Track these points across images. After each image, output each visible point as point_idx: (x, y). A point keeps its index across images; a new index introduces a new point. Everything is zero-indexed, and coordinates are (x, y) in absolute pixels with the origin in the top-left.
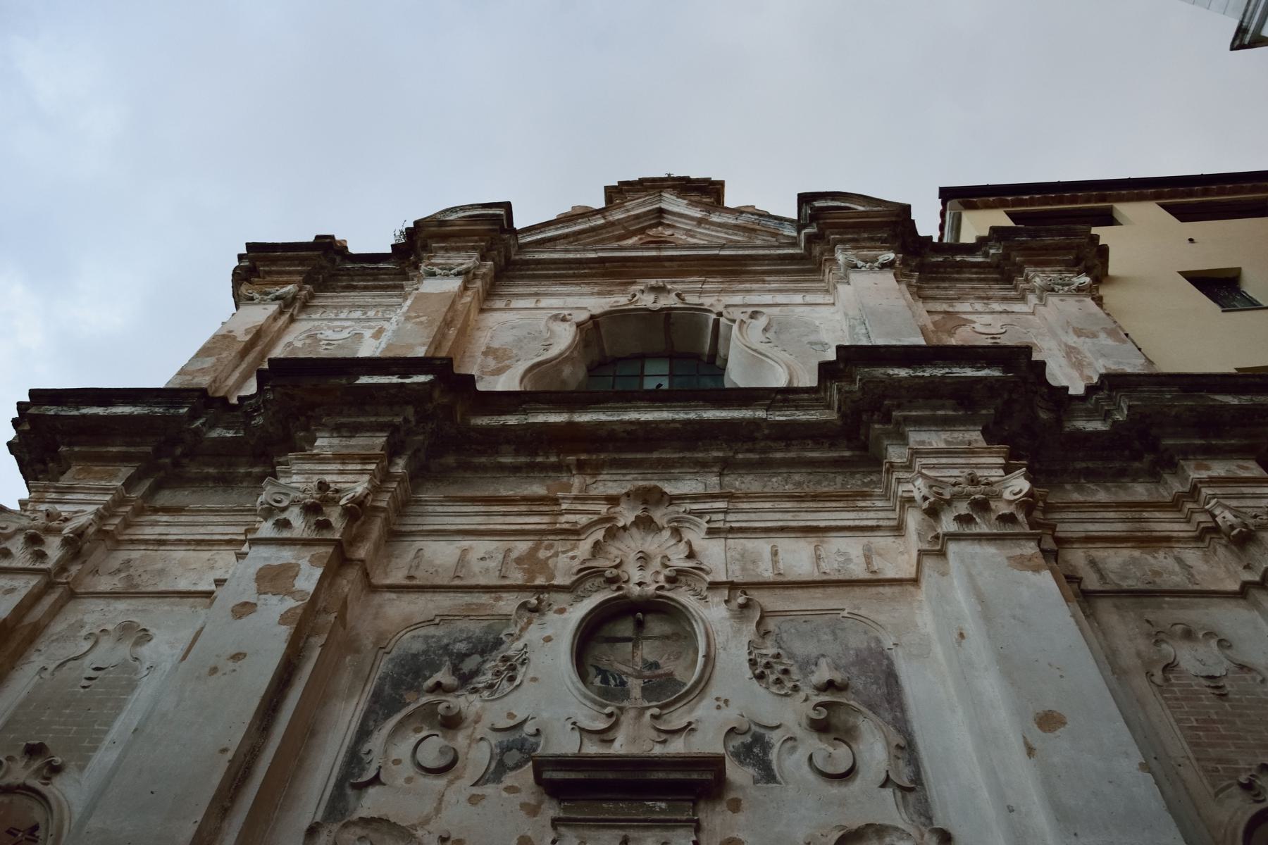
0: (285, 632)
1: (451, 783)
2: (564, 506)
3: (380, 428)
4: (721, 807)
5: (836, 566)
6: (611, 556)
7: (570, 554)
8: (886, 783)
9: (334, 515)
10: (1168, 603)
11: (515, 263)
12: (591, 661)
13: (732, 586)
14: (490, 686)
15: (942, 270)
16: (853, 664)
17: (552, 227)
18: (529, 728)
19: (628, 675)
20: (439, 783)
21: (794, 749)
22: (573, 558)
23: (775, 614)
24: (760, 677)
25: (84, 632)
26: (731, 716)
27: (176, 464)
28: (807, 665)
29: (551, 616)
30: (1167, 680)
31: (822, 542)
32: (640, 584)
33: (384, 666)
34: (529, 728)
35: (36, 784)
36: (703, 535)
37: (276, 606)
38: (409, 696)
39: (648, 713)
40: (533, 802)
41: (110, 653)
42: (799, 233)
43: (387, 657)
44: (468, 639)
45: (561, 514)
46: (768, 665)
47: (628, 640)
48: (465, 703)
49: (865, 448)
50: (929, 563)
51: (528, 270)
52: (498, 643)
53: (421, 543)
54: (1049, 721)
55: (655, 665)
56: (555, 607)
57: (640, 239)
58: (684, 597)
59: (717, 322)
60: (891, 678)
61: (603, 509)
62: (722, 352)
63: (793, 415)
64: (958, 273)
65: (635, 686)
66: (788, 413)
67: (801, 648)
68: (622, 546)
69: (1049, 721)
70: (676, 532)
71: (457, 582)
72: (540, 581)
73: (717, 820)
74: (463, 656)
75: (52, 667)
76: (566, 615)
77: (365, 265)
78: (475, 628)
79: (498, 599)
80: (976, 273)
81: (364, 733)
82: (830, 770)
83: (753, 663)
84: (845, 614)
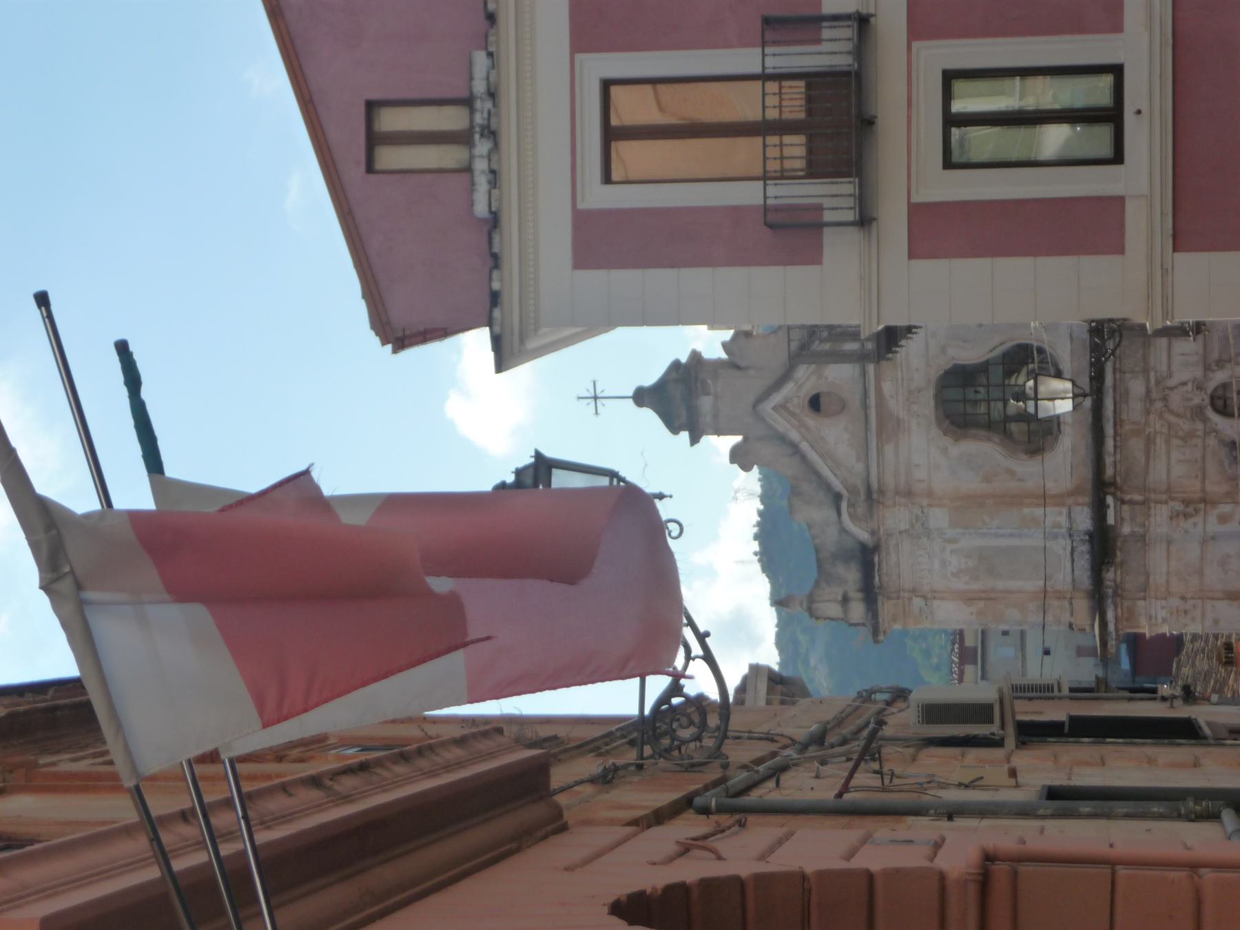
9: (1190, 510)
22: (1184, 423)
29: (1219, 427)
58: (1211, 386)
61: (1152, 417)
72: (1200, 433)
78: (1224, 452)
79: (1209, 446)
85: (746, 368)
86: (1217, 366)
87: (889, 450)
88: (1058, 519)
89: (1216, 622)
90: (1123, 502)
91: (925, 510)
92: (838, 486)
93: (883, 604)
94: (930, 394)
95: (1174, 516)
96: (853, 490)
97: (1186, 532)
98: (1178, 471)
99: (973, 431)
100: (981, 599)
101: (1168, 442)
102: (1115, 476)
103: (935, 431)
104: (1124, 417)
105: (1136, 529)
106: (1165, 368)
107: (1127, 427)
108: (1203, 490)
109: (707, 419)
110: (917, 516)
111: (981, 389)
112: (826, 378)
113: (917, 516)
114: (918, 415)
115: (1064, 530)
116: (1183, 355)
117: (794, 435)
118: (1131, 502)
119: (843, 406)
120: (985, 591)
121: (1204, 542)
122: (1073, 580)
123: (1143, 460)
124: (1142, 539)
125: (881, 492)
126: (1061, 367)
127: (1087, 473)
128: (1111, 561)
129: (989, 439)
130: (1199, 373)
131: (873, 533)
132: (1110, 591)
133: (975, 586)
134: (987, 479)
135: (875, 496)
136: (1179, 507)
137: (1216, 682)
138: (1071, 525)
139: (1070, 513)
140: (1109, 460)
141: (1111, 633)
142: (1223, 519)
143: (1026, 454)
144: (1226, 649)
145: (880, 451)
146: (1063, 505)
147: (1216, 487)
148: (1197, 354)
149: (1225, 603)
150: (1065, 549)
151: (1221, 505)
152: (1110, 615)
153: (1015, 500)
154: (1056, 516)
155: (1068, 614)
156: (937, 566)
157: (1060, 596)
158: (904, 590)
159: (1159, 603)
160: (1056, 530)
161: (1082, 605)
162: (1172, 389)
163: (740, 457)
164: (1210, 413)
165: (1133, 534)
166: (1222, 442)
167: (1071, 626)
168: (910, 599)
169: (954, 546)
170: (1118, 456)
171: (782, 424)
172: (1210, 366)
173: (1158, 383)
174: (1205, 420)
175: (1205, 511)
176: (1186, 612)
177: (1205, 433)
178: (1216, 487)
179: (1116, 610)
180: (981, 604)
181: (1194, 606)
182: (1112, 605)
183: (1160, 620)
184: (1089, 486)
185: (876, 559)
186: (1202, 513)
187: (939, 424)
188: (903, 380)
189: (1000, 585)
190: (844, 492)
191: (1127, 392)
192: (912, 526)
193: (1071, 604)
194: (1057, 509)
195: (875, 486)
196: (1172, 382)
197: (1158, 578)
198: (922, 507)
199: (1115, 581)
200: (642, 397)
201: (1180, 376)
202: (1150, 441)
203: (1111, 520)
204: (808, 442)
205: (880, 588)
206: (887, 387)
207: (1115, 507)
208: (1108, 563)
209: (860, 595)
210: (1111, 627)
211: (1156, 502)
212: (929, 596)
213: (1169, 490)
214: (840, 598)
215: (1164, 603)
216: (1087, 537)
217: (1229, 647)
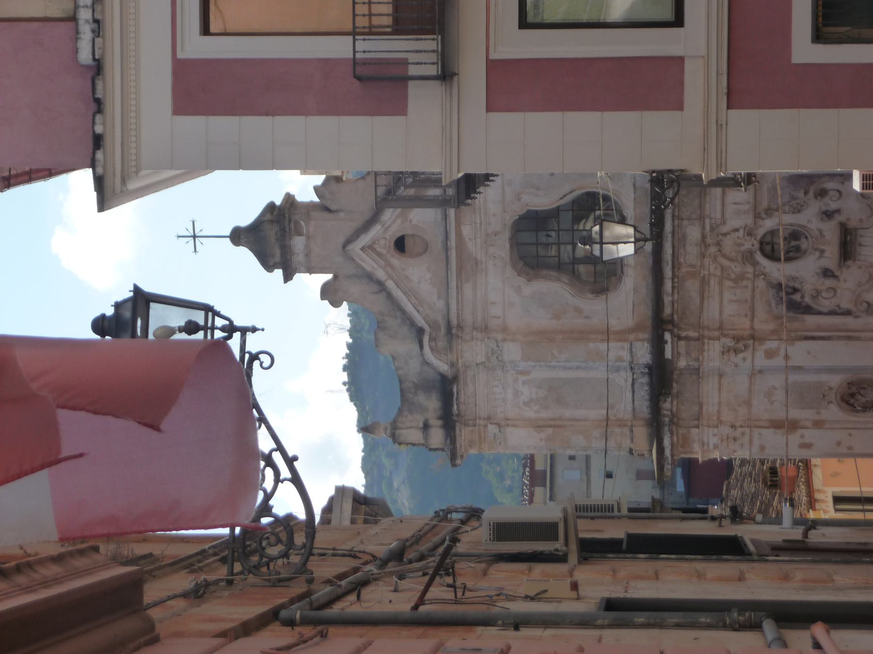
7: (733, 268)
8: (843, 183)
9: (740, 345)
20: (839, 291)
22: (736, 267)
24: (799, 211)
29: (768, 270)
47: (773, 247)
48: (808, 288)
56: (763, 269)
58: (761, 232)
61: (707, 261)
65: (793, 243)
72: (750, 276)
73: (852, 224)
78: (772, 292)
79: (758, 287)
81: (820, 313)
82: (839, 196)
83: (793, 213)
85: (337, 211)
86: (766, 214)
87: (468, 289)
88: (621, 353)
89: (762, 448)
90: (680, 338)
91: (500, 344)
92: (420, 321)
93: (460, 431)
94: (507, 235)
95: (726, 351)
96: (434, 326)
97: (736, 366)
98: (730, 309)
99: (545, 272)
100: (550, 426)
101: (721, 284)
102: (672, 315)
103: (509, 271)
104: (682, 260)
105: (691, 363)
106: (719, 216)
107: (684, 270)
108: (752, 328)
109: (299, 258)
110: (492, 349)
111: (553, 234)
112: (411, 221)
113: (492, 349)
114: (495, 257)
115: (626, 364)
116: (736, 203)
117: (381, 274)
118: (687, 338)
119: (426, 247)
121: (752, 375)
122: (634, 409)
123: (698, 300)
124: (696, 372)
125: (460, 327)
126: (625, 214)
127: (646, 311)
128: (668, 392)
129: (558, 280)
130: (749, 220)
131: (452, 365)
132: (667, 419)
133: (544, 414)
134: (557, 317)
135: (454, 331)
136: (730, 343)
137: (761, 503)
138: (633, 360)
139: (631, 348)
140: (667, 300)
141: (667, 458)
142: (770, 354)
143: (593, 293)
144: (771, 473)
145: (459, 289)
146: (625, 340)
147: (763, 325)
148: (748, 203)
149: (772, 430)
150: (626, 381)
152: (667, 442)
153: (580, 335)
154: (618, 350)
155: (629, 441)
156: (510, 396)
157: (621, 423)
158: (480, 418)
159: (711, 430)
160: (618, 364)
161: (642, 433)
162: (725, 235)
163: (330, 294)
164: (759, 257)
165: (688, 368)
167: (631, 451)
168: (485, 426)
169: (525, 378)
170: (676, 296)
171: (369, 263)
172: (759, 214)
173: (712, 229)
174: (755, 264)
175: (754, 349)
176: (735, 439)
177: (754, 276)
178: (763, 325)
179: (672, 437)
180: (550, 431)
181: (743, 434)
182: (668, 433)
183: (711, 446)
184: (649, 323)
185: (455, 390)
186: (751, 349)
187: (514, 266)
188: (481, 224)
189: (568, 413)
190: (427, 328)
191: (684, 237)
192: (488, 359)
193: (632, 431)
194: (619, 344)
195: (454, 322)
196: (725, 229)
197: (710, 409)
198: (496, 341)
199: (671, 410)
200: (238, 236)
202: (704, 282)
203: (668, 354)
204: (394, 281)
205: (458, 415)
206: (466, 230)
207: (672, 343)
208: (666, 393)
209: (440, 423)
210: (668, 453)
211: (710, 338)
212: (503, 423)
213: (721, 328)
214: (421, 425)
215: (715, 430)
216: (647, 370)
217: (773, 471)
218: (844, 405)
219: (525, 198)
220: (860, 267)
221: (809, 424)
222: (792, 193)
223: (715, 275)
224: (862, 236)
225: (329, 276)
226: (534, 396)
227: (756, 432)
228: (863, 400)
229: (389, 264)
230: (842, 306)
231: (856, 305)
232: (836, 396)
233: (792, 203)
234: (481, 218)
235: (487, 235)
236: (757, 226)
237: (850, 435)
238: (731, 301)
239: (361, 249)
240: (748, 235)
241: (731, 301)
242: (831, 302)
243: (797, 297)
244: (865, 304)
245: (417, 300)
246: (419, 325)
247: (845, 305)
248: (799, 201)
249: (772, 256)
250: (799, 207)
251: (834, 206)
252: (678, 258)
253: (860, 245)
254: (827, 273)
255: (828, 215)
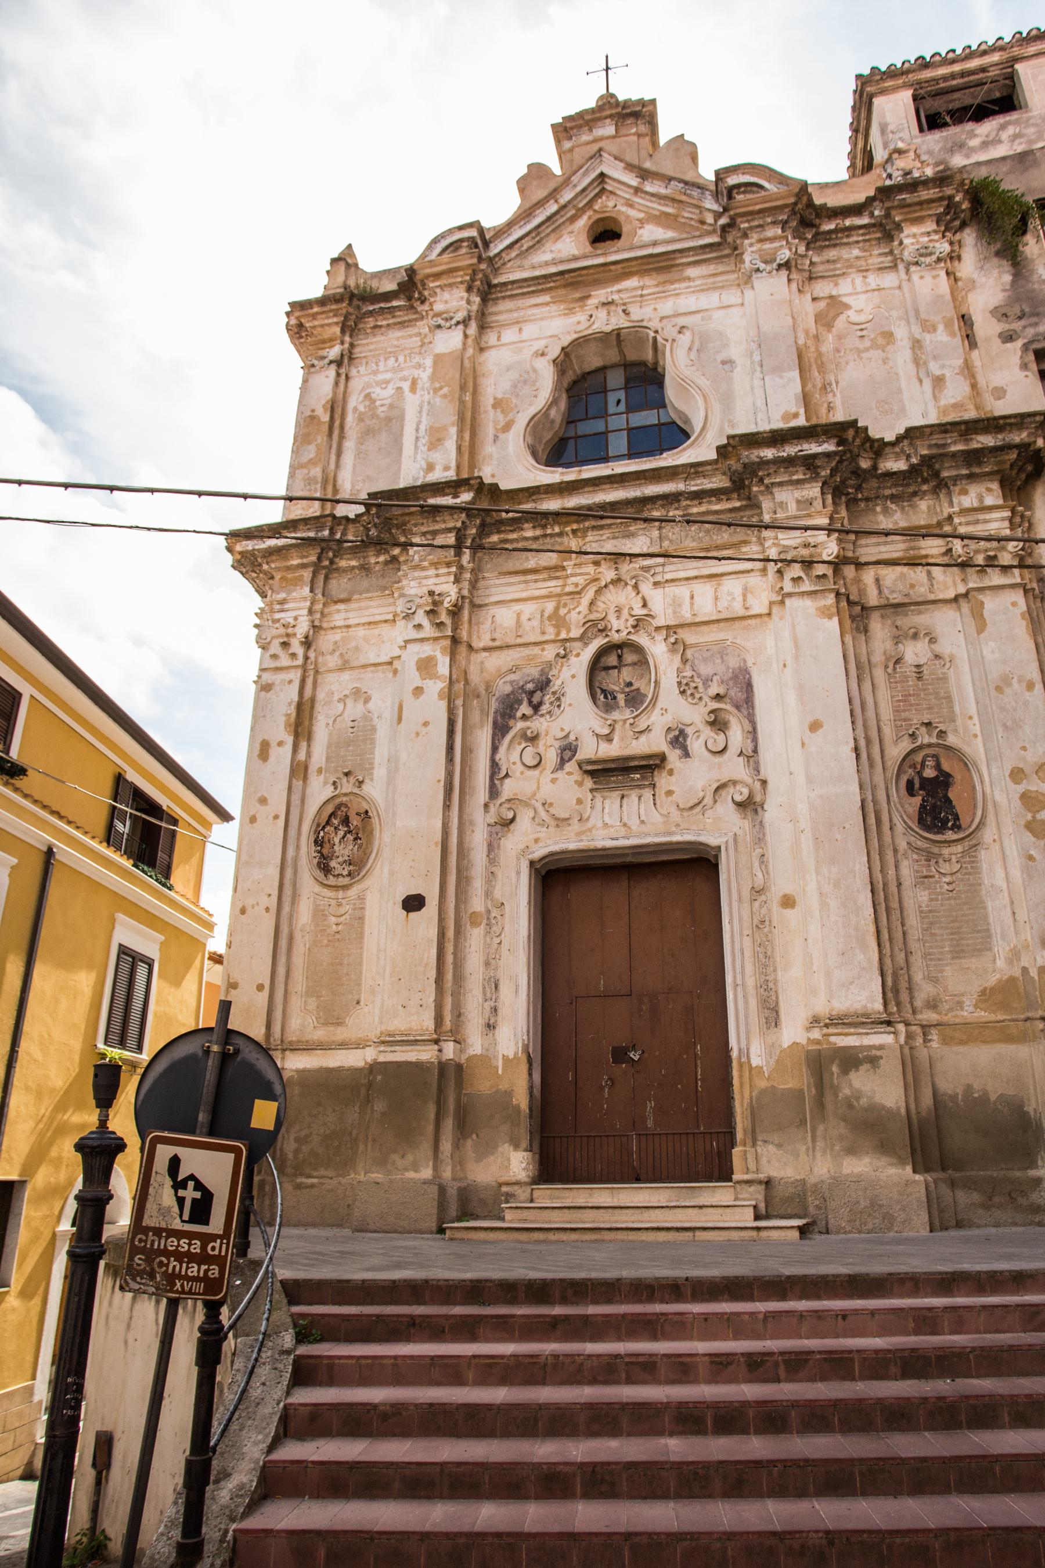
0: (443, 704)
1: (541, 772)
2: (569, 572)
3: (450, 530)
4: (664, 774)
5: (726, 605)
6: (600, 609)
7: (577, 610)
8: (741, 754)
9: (444, 617)
10: (912, 611)
11: (496, 286)
12: (597, 684)
13: (668, 628)
14: (549, 712)
15: (834, 236)
16: (731, 679)
17: (516, 227)
18: (572, 737)
19: (618, 692)
20: (535, 773)
21: (698, 737)
22: (579, 613)
23: (692, 646)
24: (683, 692)
25: (336, 698)
26: (668, 720)
27: (332, 562)
28: (707, 681)
29: (573, 659)
30: (895, 669)
31: (719, 584)
32: (618, 631)
33: (494, 705)
34: (572, 737)
35: (356, 790)
36: (651, 586)
37: (435, 687)
38: (511, 723)
39: (629, 722)
40: (580, 779)
41: (354, 710)
42: (716, 221)
43: (494, 699)
44: (532, 680)
45: (567, 577)
46: (687, 684)
47: (615, 667)
48: (538, 724)
49: (749, 498)
50: (775, 609)
51: (507, 290)
52: (548, 682)
53: (494, 610)
54: (815, 726)
55: (630, 684)
56: (574, 653)
57: (590, 218)
58: (641, 639)
59: (655, 339)
60: (749, 687)
62: (661, 363)
63: (702, 484)
64: (848, 236)
65: (621, 698)
66: (699, 482)
67: (705, 670)
68: (606, 600)
69: (815, 726)
70: (636, 587)
71: (519, 641)
73: (663, 780)
74: (531, 693)
75: (331, 722)
76: (581, 657)
77: (382, 305)
78: (534, 672)
79: (543, 650)
80: (862, 235)
81: (495, 749)
83: (679, 683)
84: (728, 643)
98: (505, 617)
100: (332, 418)
106: (668, 576)
111: (622, 407)
112: (640, 228)
113: (451, 318)
114: (591, 316)
116: (692, 597)
120: (342, 428)
130: (661, 621)
133: (350, 419)
149: (296, 698)
151: (447, 659)
159: (305, 612)
162: (636, 587)
166: (550, 665)
172: (675, 633)
173: (646, 569)
174: (584, 639)
175: (436, 639)
177: (566, 640)
180: (326, 418)
181: (294, 655)
183: (277, 616)
189: (349, 445)
194: (453, 464)
196: (646, 588)
201: (658, 600)
206: (633, 282)
218: (330, 809)
219: (685, 339)
220: (579, 802)
221: (302, 756)
222: (715, 678)
223: (565, 585)
224: (640, 798)
225: (557, 171)
226: (378, 403)
227: (296, 676)
228: (337, 840)
229: (581, 212)
230: (507, 781)
231: (509, 801)
232: (345, 795)
233: (697, 680)
234: (650, 294)
235: (624, 304)
236: (653, 634)
237: (276, 817)
238: (519, 615)
239: (602, 175)
240: (637, 620)
241: (519, 615)
242: (514, 763)
243: (525, 709)
244: (510, 815)
245: (527, 250)
246: (492, 245)
247: (508, 789)
248: (701, 689)
249: (596, 666)
250: (689, 692)
251: (695, 745)
252: (594, 528)
253: (623, 797)
254: (568, 750)
255: (679, 739)
